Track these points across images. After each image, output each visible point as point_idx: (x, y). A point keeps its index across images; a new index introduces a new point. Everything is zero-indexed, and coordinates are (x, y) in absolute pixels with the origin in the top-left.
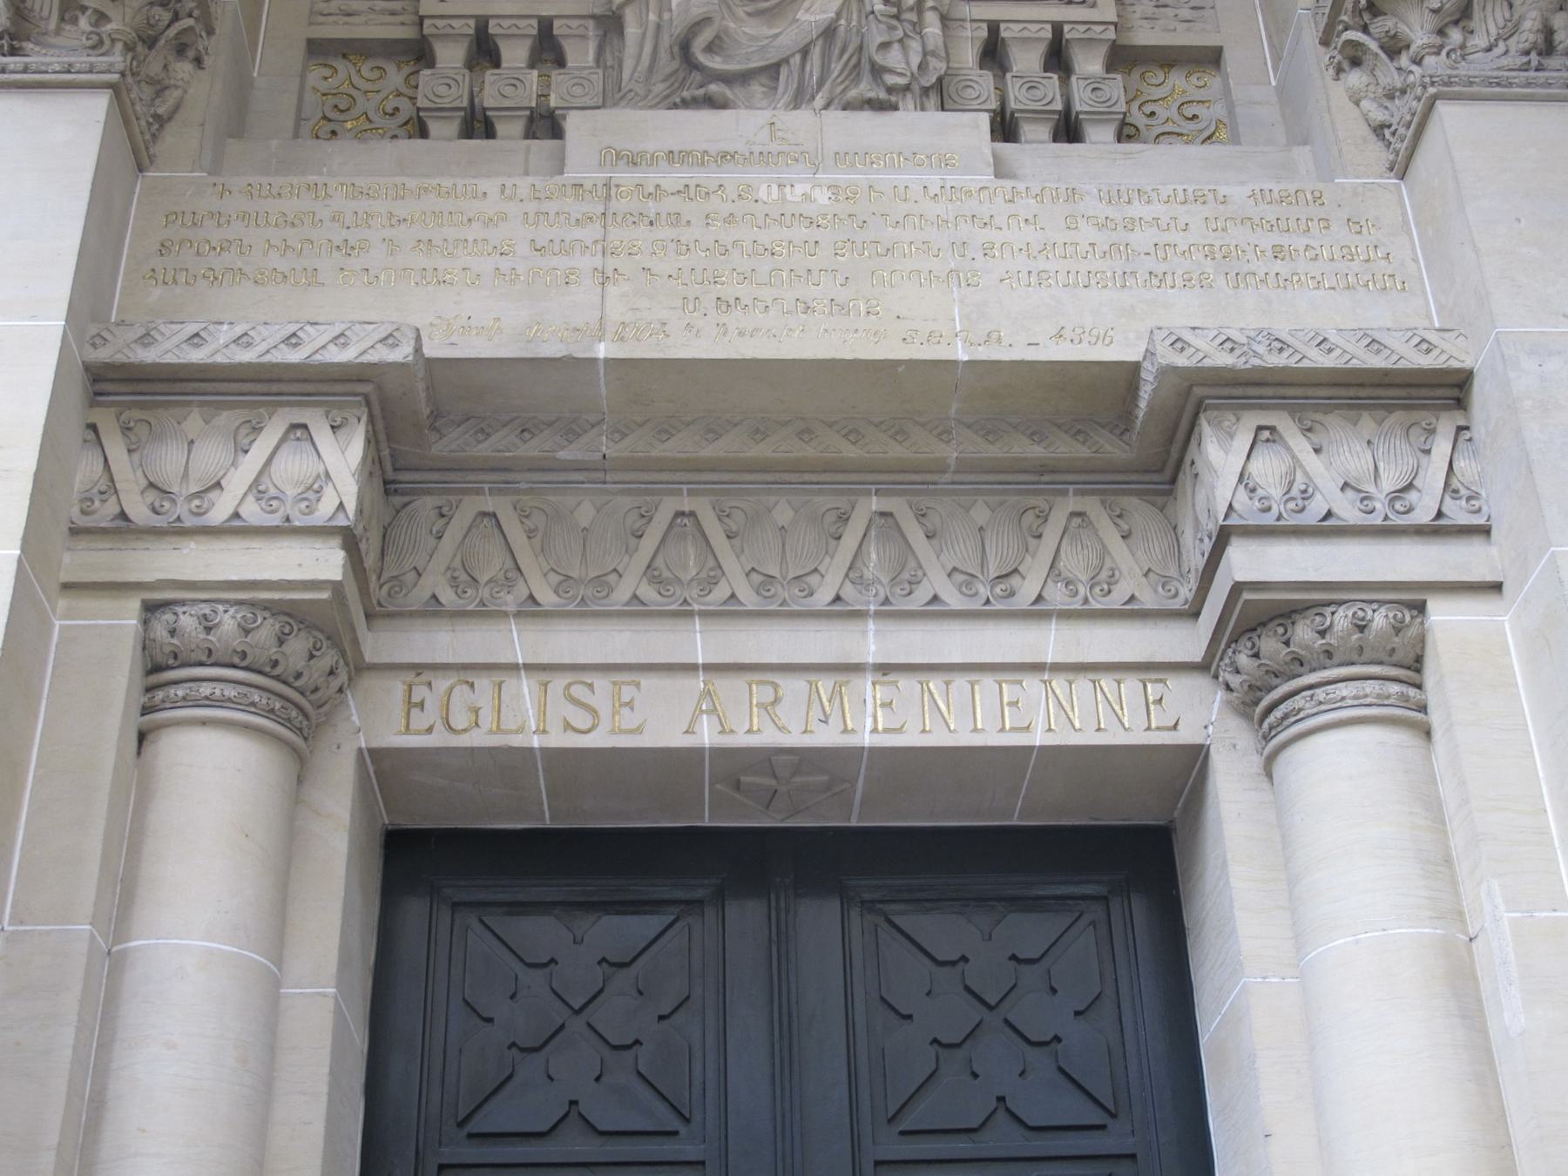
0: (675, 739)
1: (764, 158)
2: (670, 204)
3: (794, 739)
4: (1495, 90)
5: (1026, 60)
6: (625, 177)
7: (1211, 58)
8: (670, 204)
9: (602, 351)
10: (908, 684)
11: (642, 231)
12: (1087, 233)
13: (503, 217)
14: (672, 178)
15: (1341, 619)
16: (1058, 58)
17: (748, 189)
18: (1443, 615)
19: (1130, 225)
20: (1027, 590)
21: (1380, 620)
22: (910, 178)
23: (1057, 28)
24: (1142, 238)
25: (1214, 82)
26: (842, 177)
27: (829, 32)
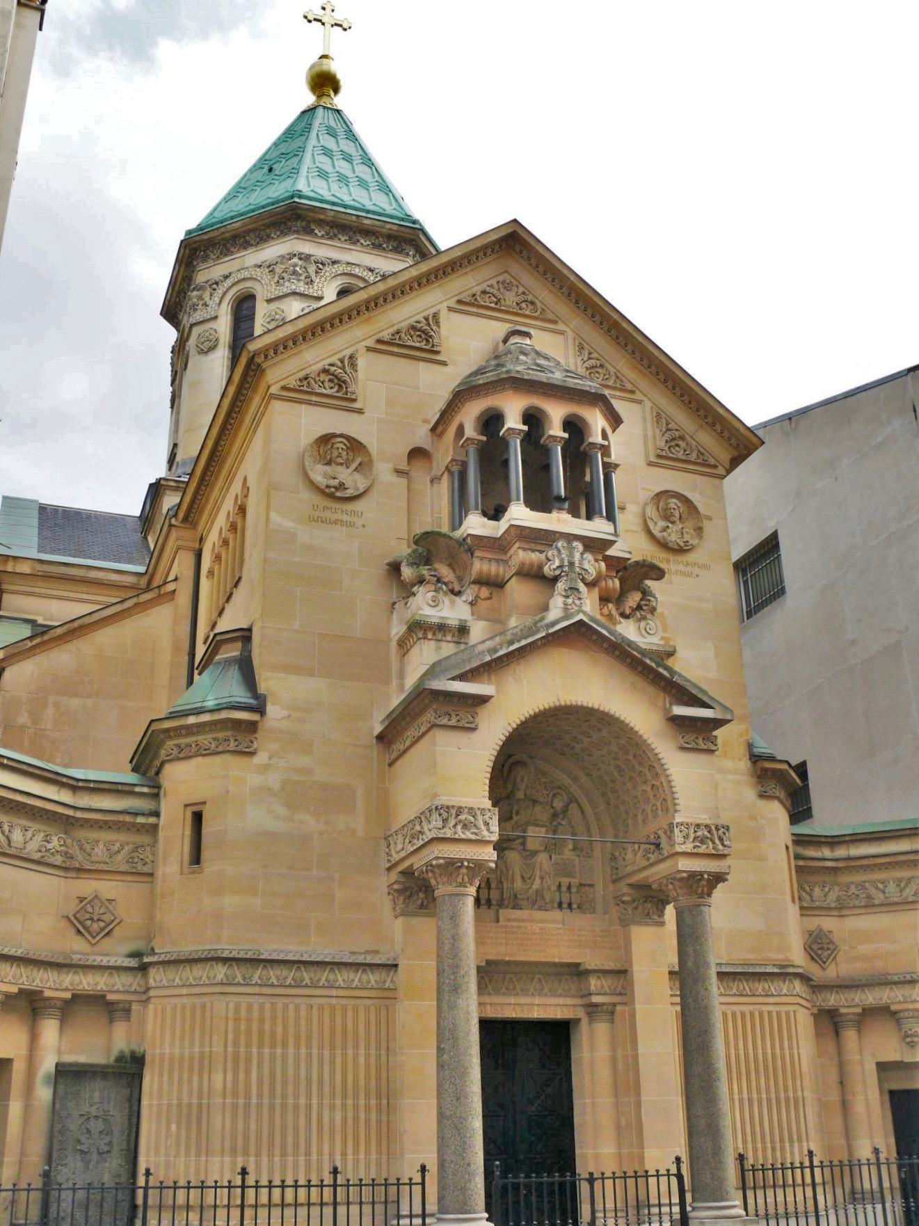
0: (510, 1016)
1: (528, 921)
2: (515, 930)
3: (526, 1016)
4: (639, 923)
5: (564, 889)
6: (509, 924)
7: (592, 885)
8: (515, 930)
9: (507, 959)
10: (541, 1007)
11: (511, 935)
12: (576, 937)
13: (490, 931)
14: (515, 924)
15: (605, 1007)
16: (569, 887)
17: (526, 928)
18: (619, 1008)
19: (582, 935)
20: (560, 991)
21: (610, 1007)
22: (550, 926)
23: (570, 883)
24: (583, 938)
25: (592, 889)
26: (540, 925)
27: (537, 891)
